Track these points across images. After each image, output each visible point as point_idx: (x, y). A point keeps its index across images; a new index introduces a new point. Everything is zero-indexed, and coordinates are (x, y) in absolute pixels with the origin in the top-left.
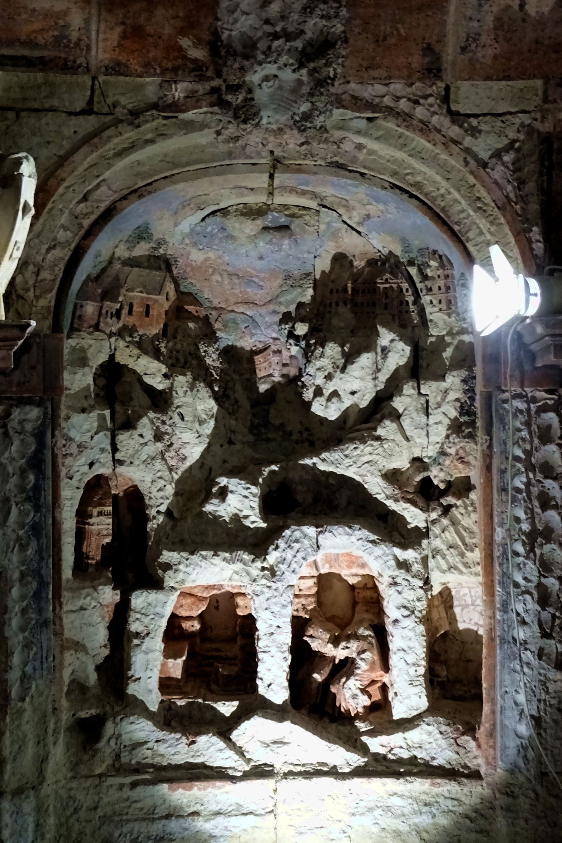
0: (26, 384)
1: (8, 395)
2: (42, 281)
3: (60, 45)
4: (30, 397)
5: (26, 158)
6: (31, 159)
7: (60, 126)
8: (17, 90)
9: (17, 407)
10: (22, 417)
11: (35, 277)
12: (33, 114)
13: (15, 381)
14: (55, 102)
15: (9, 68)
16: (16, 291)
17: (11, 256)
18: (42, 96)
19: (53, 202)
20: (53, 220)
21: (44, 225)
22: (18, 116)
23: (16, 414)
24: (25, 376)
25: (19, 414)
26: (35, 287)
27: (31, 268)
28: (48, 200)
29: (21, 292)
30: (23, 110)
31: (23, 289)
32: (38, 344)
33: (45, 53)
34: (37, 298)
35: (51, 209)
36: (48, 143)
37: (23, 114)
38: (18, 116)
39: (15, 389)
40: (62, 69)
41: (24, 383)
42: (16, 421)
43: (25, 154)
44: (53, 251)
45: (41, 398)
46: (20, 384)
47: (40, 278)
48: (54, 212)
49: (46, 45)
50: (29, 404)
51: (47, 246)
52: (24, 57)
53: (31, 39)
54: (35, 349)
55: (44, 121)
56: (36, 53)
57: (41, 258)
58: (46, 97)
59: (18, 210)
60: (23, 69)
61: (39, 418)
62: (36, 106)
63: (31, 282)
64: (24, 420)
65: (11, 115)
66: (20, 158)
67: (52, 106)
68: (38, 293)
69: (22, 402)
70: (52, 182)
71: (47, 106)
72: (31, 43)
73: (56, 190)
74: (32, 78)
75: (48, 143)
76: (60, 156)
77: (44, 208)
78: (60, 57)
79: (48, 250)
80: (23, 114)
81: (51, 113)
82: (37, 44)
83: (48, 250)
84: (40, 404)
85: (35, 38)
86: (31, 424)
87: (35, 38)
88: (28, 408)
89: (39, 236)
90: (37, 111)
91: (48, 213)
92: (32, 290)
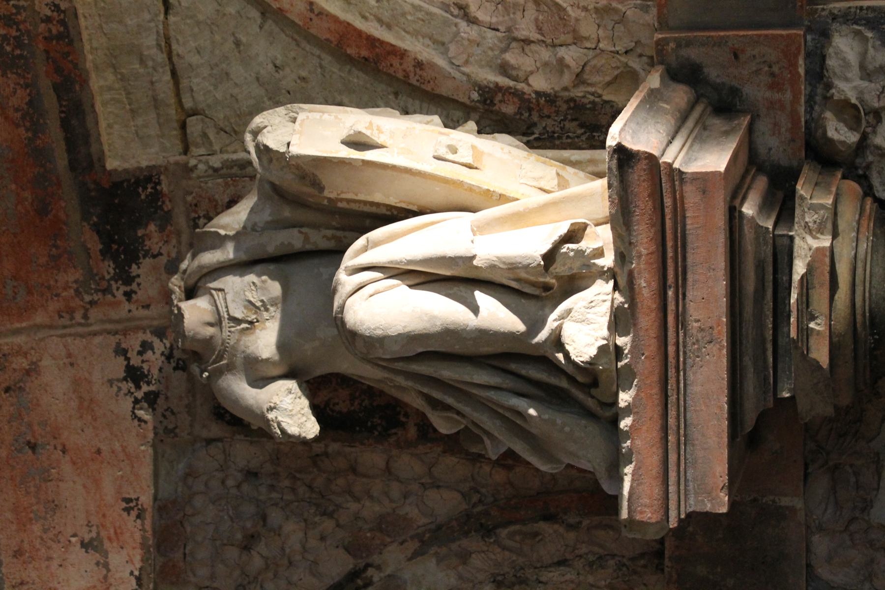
0: (776, 69)
1: (802, 110)
2: (540, 30)
3: (21, 57)
4: (808, 55)
5: (256, 133)
6: (258, 120)
7: (198, 23)
8: (140, 121)
9: (829, 86)
10: (854, 72)
11: (533, 47)
12: (184, 83)
13: (768, 94)
14: (149, 42)
15: (94, 149)
16: (566, 89)
17: (470, 167)
18: (141, 71)
19: (364, 17)
20: (404, 14)
21: (416, 34)
22: (194, 113)
23: (848, 87)
24: (757, 72)
25: (847, 80)
26: (554, 46)
27: (510, 57)
28: (359, 33)
29: (567, 79)
30: (180, 103)
31: (562, 73)
32: (679, 46)
33: (45, 84)
34: (578, 39)
35: (380, 21)
36: (238, 43)
37: (188, 103)
38: (194, 113)
39: (788, 96)
40: (71, 43)
41: (773, 75)
42: (865, 84)
43: (248, 137)
44: (473, 9)
45: (809, 30)
46: (775, 85)
47: (535, 36)
48: (386, 16)
49: (27, 86)
50: (823, 58)
51: (463, 24)
52: (65, 124)
53: (23, 118)
54: (694, 54)
55: (195, 59)
56: (50, 101)
57: (490, 34)
58: (142, 62)
59: (366, 163)
60: (90, 124)
61: (857, 33)
62: (168, 77)
63: (545, 54)
64: (862, 67)
65: (195, 126)
66: (257, 147)
67: (159, 45)
68: (569, 38)
69: (819, 74)
70: (319, 29)
71: (161, 57)
72: (32, 114)
73: (336, 19)
74: (107, 96)
75: (238, 43)
76: (263, 14)
77: (382, 43)
78: (47, 52)
79: (473, 21)
80: (188, 103)
81: (174, 47)
82: (30, 103)
83: (473, 21)
84: (825, 35)
85: (16, 110)
86: (871, 51)
87: (16, 110)
88: (832, 62)
89: (443, 44)
90: (174, 73)
91: (389, 27)
92: (562, 52)
